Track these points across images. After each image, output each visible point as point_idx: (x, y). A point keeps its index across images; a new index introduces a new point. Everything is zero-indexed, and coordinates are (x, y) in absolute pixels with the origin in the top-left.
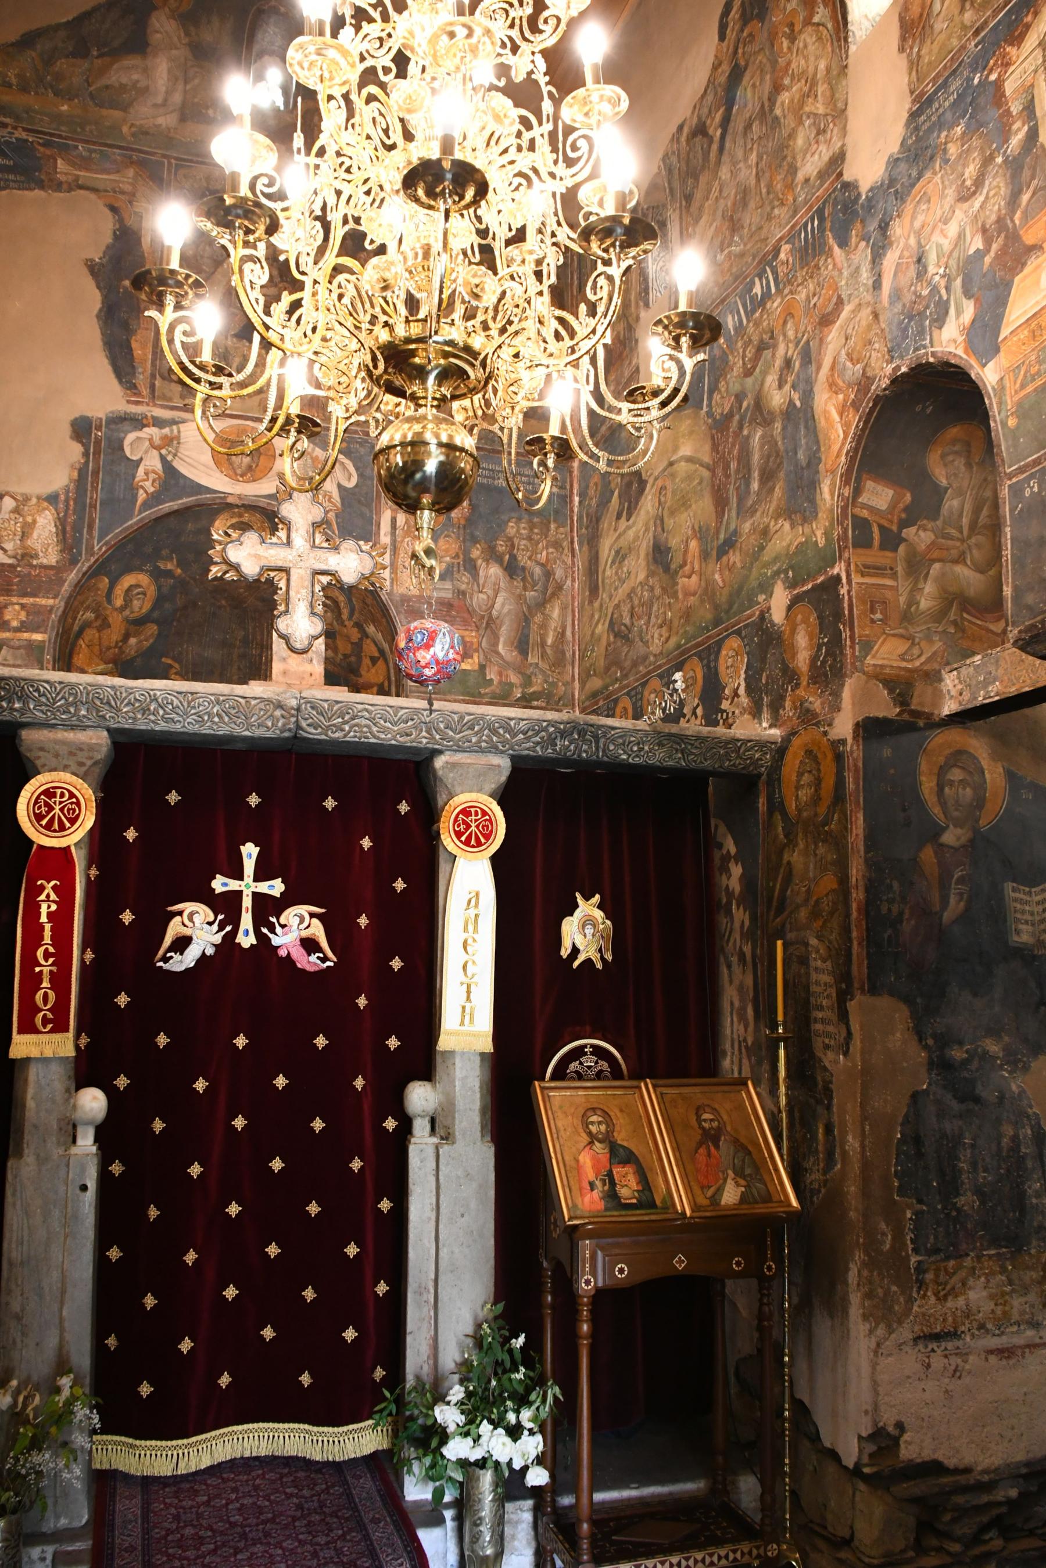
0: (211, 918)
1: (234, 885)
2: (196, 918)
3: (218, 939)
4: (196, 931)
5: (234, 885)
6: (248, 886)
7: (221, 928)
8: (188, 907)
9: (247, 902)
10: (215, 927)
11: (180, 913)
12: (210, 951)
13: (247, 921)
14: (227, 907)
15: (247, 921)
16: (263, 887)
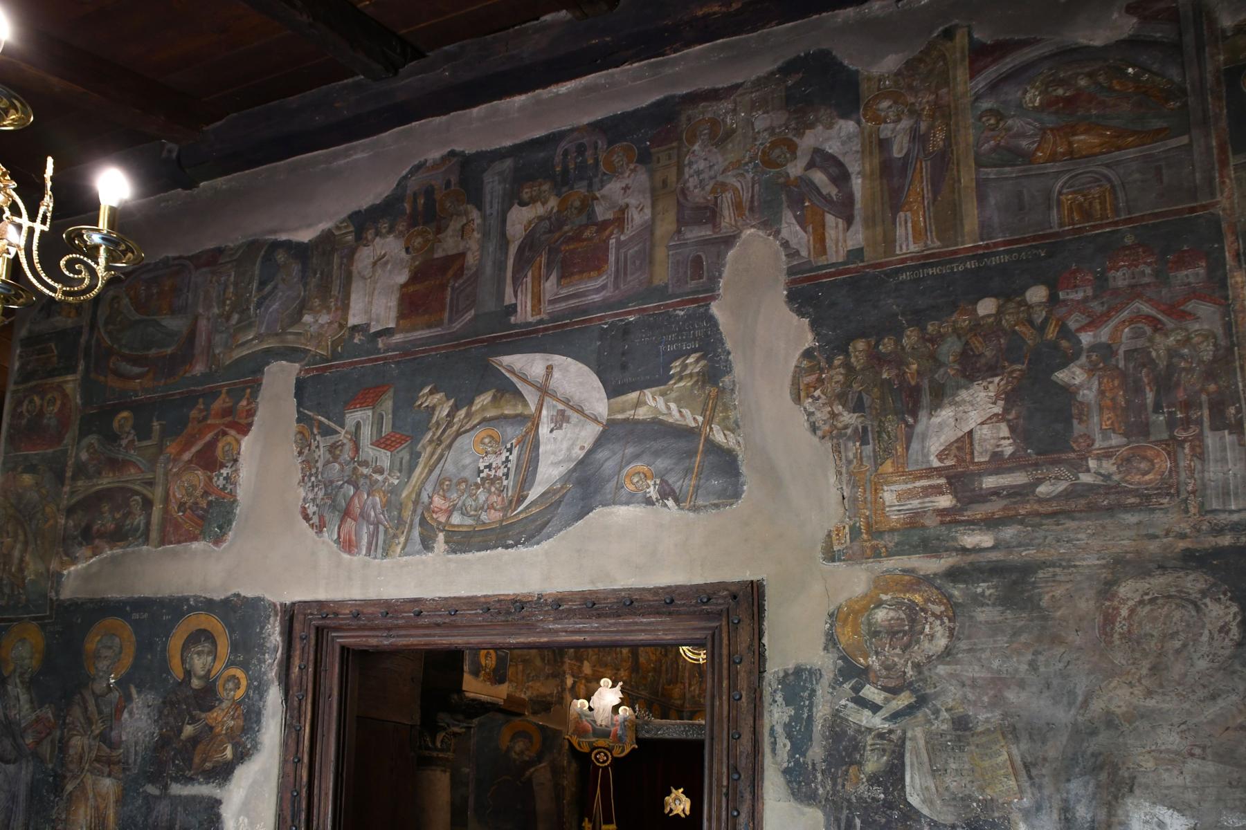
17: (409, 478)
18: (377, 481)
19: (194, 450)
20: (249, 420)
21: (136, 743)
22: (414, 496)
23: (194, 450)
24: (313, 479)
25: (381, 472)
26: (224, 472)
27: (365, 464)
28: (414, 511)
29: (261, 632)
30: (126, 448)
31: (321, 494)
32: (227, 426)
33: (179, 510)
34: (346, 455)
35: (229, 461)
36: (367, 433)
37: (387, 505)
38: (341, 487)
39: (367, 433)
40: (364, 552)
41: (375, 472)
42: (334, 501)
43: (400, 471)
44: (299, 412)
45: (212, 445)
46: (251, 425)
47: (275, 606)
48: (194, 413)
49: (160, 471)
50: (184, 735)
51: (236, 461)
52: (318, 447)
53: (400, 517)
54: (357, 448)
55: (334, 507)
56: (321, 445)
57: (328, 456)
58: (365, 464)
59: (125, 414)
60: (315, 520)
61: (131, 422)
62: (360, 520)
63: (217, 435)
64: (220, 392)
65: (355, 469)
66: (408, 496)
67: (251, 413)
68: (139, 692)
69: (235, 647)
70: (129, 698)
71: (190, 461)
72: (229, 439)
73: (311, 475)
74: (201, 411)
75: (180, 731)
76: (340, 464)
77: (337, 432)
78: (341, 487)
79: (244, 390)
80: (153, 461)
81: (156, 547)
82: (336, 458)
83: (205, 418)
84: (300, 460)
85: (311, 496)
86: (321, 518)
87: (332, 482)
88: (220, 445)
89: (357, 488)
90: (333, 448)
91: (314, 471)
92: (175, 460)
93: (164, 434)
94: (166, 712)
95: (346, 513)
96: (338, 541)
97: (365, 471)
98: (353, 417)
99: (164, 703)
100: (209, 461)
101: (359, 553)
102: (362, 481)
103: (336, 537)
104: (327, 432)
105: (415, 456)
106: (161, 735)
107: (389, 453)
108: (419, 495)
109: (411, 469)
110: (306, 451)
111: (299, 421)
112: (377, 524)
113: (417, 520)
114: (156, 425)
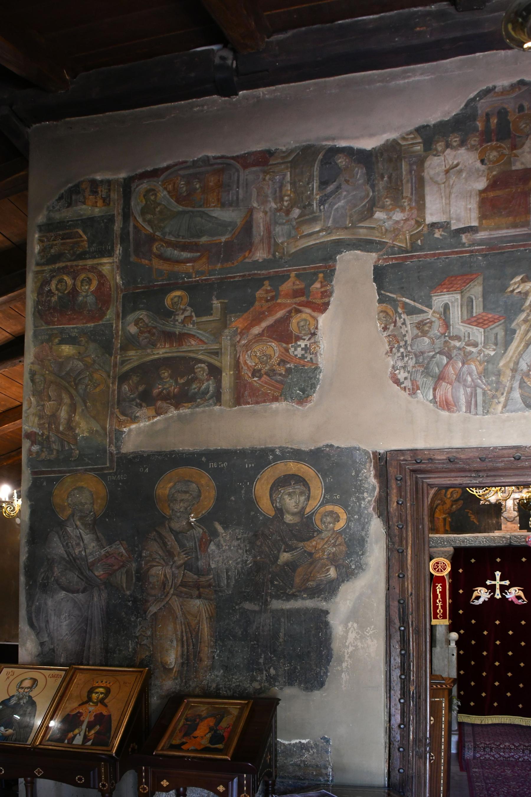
0: (487, 591)
1: (493, 582)
2: (482, 591)
3: (489, 596)
4: (482, 594)
5: (493, 582)
6: (498, 583)
7: (490, 593)
8: (479, 589)
9: (498, 587)
10: (488, 593)
11: (477, 590)
12: (487, 600)
13: (498, 591)
14: (492, 588)
15: (498, 591)
16: (503, 583)
17: (506, 350)
18: (471, 353)
19: (264, 325)
20: (326, 300)
21: (227, 571)
22: (512, 365)
23: (264, 325)
24: (402, 350)
25: (475, 345)
26: (302, 343)
27: (458, 338)
28: (513, 377)
29: (357, 475)
30: (183, 322)
31: (412, 363)
32: (300, 304)
33: (253, 375)
34: (437, 329)
35: (305, 335)
36: (456, 314)
37: (485, 373)
38: (433, 357)
39: (456, 314)
40: (464, 409)
41: (468, 345)
42: (427, 368)
43: (496, 344)
44: (379, 294)
45: (286, 320)
46: (327, 304)
47: (368, 452)
48: (259, 293)
49: (226, 341)
50: (280, 561)
51: (314, 334)
52: (404, 323)
53: (498, 382)
54: (447, 325)
55: (427, 372)
56: (408, 322)
57: (416, 331)
58: (458, 338)
59: (178, 293)
60: (408, 384)
61: (186, 300)
62: (456, 384)
63: (290, 312)
64: (289, 277)
65: (446, 342)
66: (506, 365)
67: (327, 294)
68: (225, 528)
69: (328, 490)
70: (214, 534)
71: (261, 335)
72: (304, 316)
73: (400, 347)
74: (267, 292)
75: (277, 558)
76: (430, 338)
77: (423, 312)
78: (433, 357)
79: (316, 274)
80: (217, 335)
81: (230, 407)
82: (425, 333)
83: (273, 298)
84: (385, 334)
85: (400, 364)
86: (413, 382)
87: (422, 353)
88: (294, 321)
89: (450, 357)
90: (420, 326)
91: (402, 343)
92: (242, 334)
93: (226, 311)
94: (259, 543)
95: (440, 378)
96: (434, 401)
97: (458, 344)
98: (440, 300)
99: (256, 535)
100: (282, 333)
101: (459, 410)
102: (455, 352)
103: (431, 397)
104: (411, 311)
105: (510, 334)
106: (255, 563)
107: (482, 330)
108: (517, 363)
109: (507, 344)
110: (392, 327)
111: (380, 301)
112: (476, 386)
113: (516, 384)
114: (216, 303)
